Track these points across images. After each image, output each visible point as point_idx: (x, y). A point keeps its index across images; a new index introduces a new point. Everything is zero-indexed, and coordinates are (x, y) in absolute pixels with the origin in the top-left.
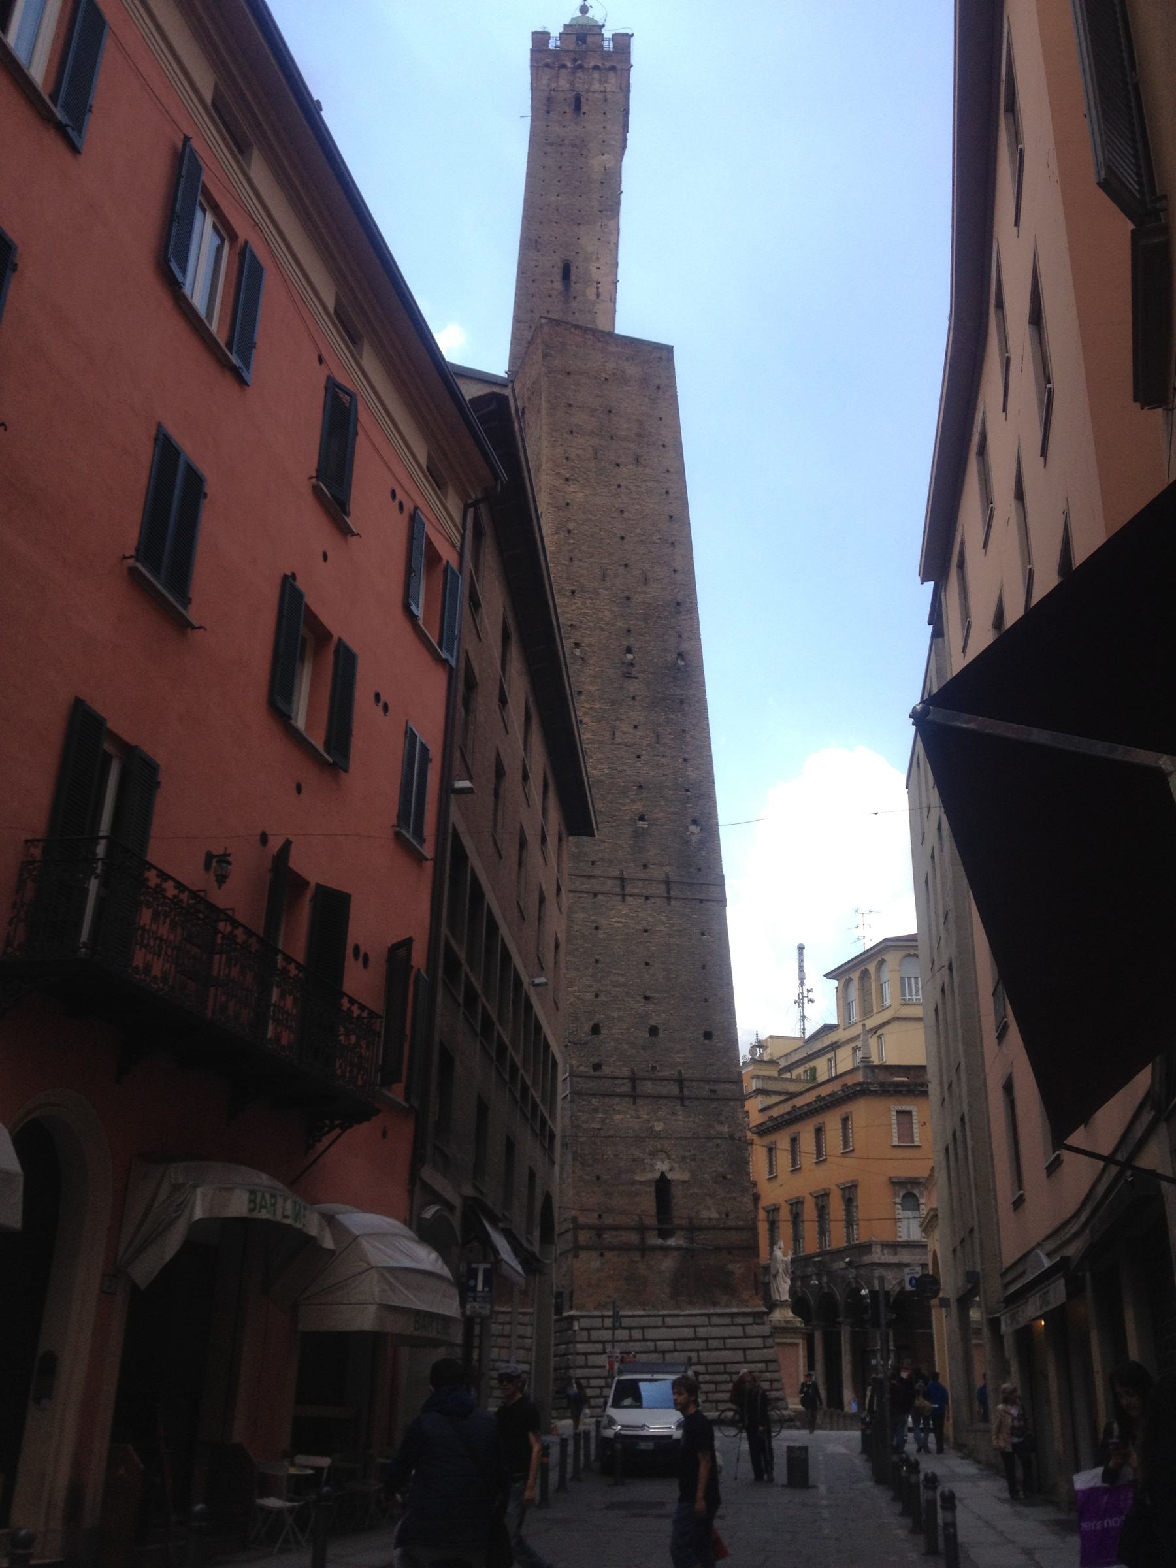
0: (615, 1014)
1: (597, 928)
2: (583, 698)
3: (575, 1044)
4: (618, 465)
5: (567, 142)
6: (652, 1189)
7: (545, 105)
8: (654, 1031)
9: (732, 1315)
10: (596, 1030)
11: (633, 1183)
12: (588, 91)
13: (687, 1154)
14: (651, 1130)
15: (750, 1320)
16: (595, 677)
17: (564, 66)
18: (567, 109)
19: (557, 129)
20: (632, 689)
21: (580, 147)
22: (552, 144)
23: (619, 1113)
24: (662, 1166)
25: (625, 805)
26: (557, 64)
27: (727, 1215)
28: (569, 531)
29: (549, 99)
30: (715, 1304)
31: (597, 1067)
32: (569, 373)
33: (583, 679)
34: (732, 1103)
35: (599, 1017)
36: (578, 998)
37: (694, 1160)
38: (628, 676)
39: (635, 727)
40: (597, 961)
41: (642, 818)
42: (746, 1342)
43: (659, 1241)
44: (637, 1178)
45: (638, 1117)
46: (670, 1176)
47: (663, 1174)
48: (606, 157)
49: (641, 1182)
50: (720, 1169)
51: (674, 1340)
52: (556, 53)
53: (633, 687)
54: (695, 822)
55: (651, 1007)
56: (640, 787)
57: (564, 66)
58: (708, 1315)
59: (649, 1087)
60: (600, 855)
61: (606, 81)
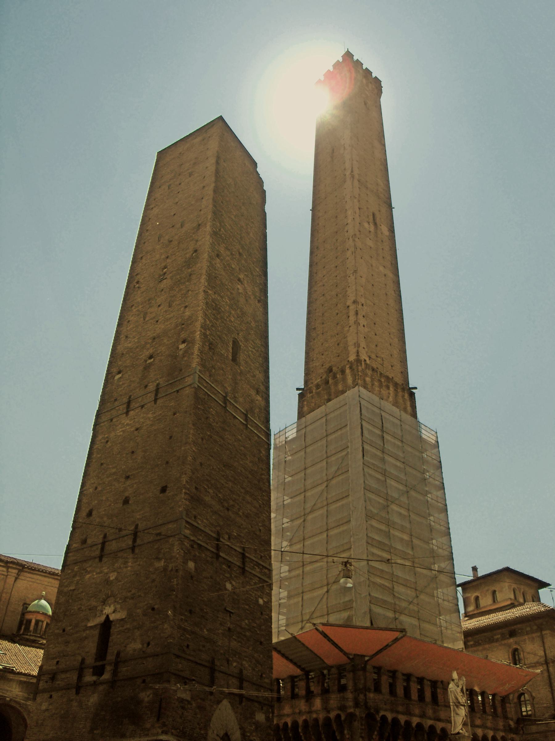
1: (107, 442)
2: (133, 308)
6: (96, 632)
8: (126, 501)
13: (129, 594)
14: (107, 582)
25: (141, 355)
27: (148, 644)
37: (132, 598)
39: (159, 306)
40: (102, 464)
41: (151, 357)
44: (90, 624)
45: (101, 572)
47: (108, 616)
50: (151, 602)
53: (163, 285)
55: (128, 482)
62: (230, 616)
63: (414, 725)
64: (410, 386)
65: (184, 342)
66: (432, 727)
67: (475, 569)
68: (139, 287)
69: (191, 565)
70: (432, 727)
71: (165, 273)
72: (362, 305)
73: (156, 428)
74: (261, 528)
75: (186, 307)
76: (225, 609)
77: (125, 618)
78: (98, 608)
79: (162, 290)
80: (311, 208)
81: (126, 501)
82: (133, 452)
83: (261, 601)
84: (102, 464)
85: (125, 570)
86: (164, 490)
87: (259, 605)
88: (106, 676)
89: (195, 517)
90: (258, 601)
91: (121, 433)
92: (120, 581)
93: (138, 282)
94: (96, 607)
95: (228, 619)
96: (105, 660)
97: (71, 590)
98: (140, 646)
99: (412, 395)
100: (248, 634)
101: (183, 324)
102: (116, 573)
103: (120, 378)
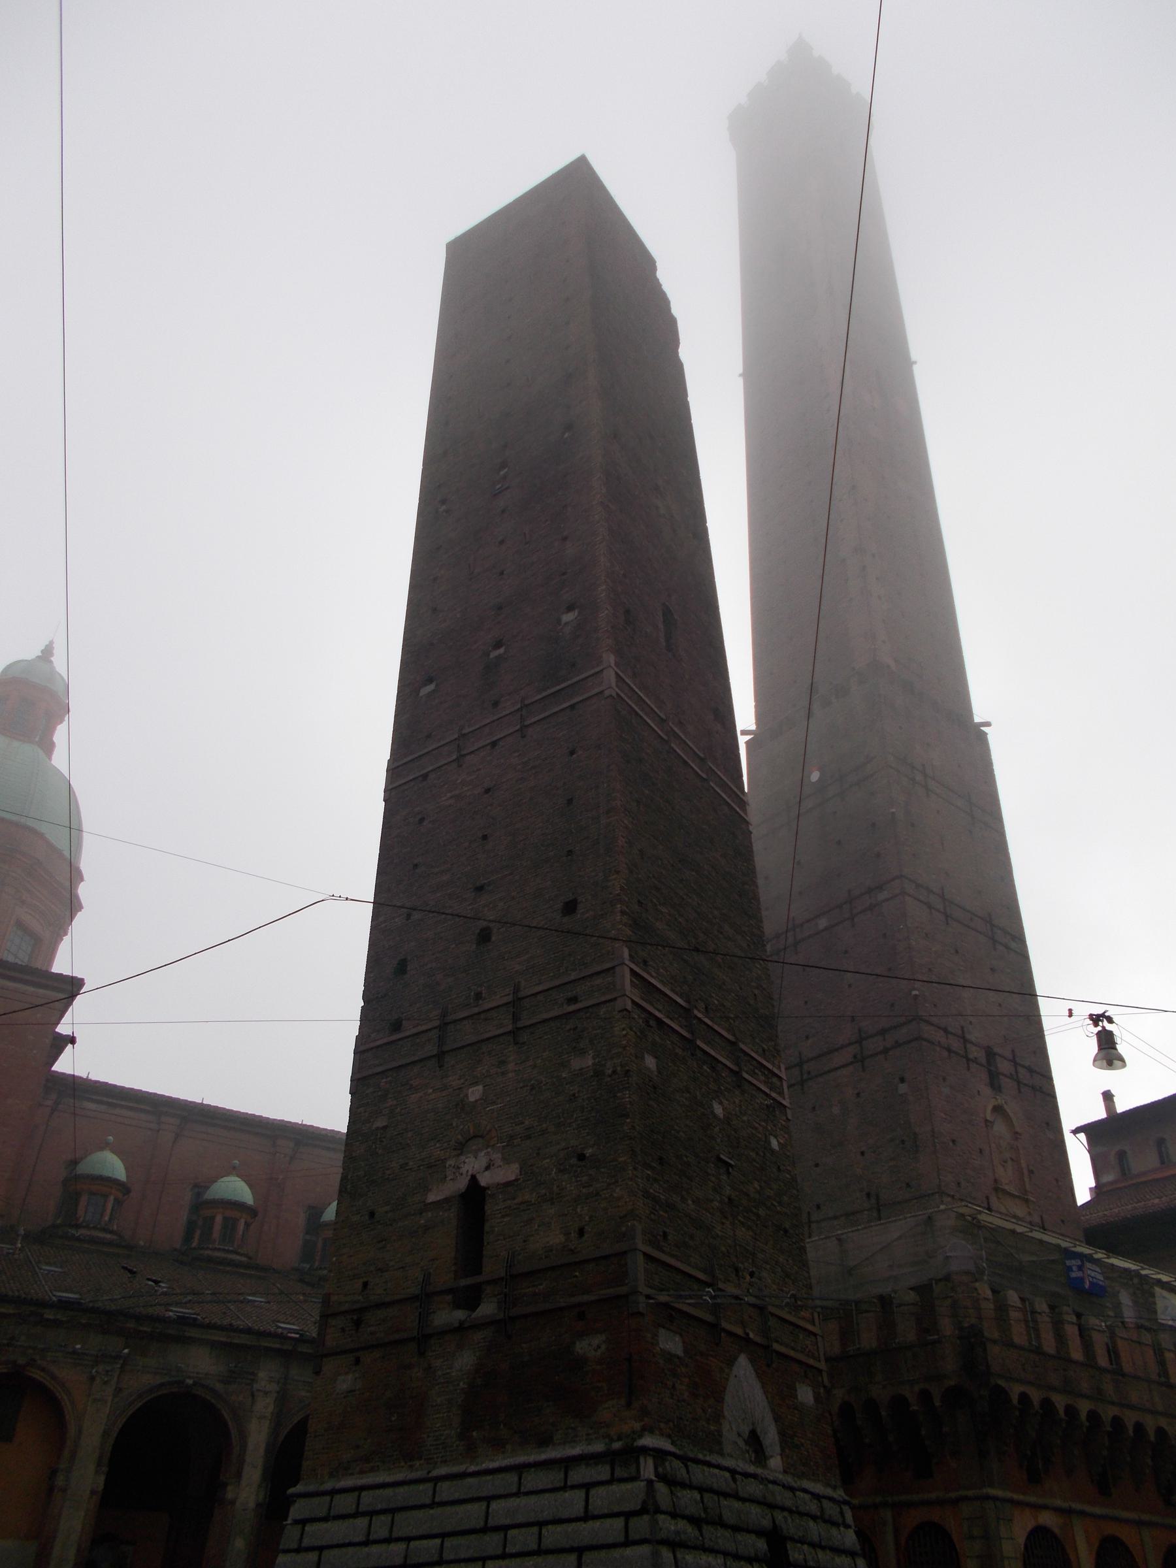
1: (422, 820)
8: (484, 937)
9: (567, 1463)
15: (602, 1472)
24: (472, 1164)
27: (581, 1232)
30: (545, 1441)
34: (602, 1011)
37: (529, 1137)
39: (502, 542)
40: (416, 866)
41: (498, 645)
42: (586, 1532)
43: (460, 1315)
44: (432, 1197)
46: (483, 1183)
47: (473, 1178)
49: (437, 1204)
58: (520, 1469)
62: (729, 1173)
63: (1083, 1416)
64: (977, 720)
65: (570, 609)
66: (1117, 1422)
67: (1108, 1097)
68: (447, 511)
69: (650, 1062)
70: (1117, 1422)
71: (505, 477)
72: (874, 556)
74: (756, 992)
75: (565, 539)
76: (719, 1159)
77: (516, 1180)
78: (448, 1163)
79: (503, 511)
80: (741, 371)
81: (484, 937)
82: (485, 837)
83: (774, 1144)
84: (416, 866)
86: (570, 907)
87: (773, 1151)
88: (487, 1309)
89: (645, 962)
90: (769, 1143)
92: (494, 1103)
93: (443, 502)
94: (444, 1161)
95: (724, 1177)
96: (480, 1273)
97: (377, 1128)
98: (562, 1238)
99: (982, 739)
100: (762, 1212)
101: (564, 574)
102: (480, 1088)
103: (434, 691)
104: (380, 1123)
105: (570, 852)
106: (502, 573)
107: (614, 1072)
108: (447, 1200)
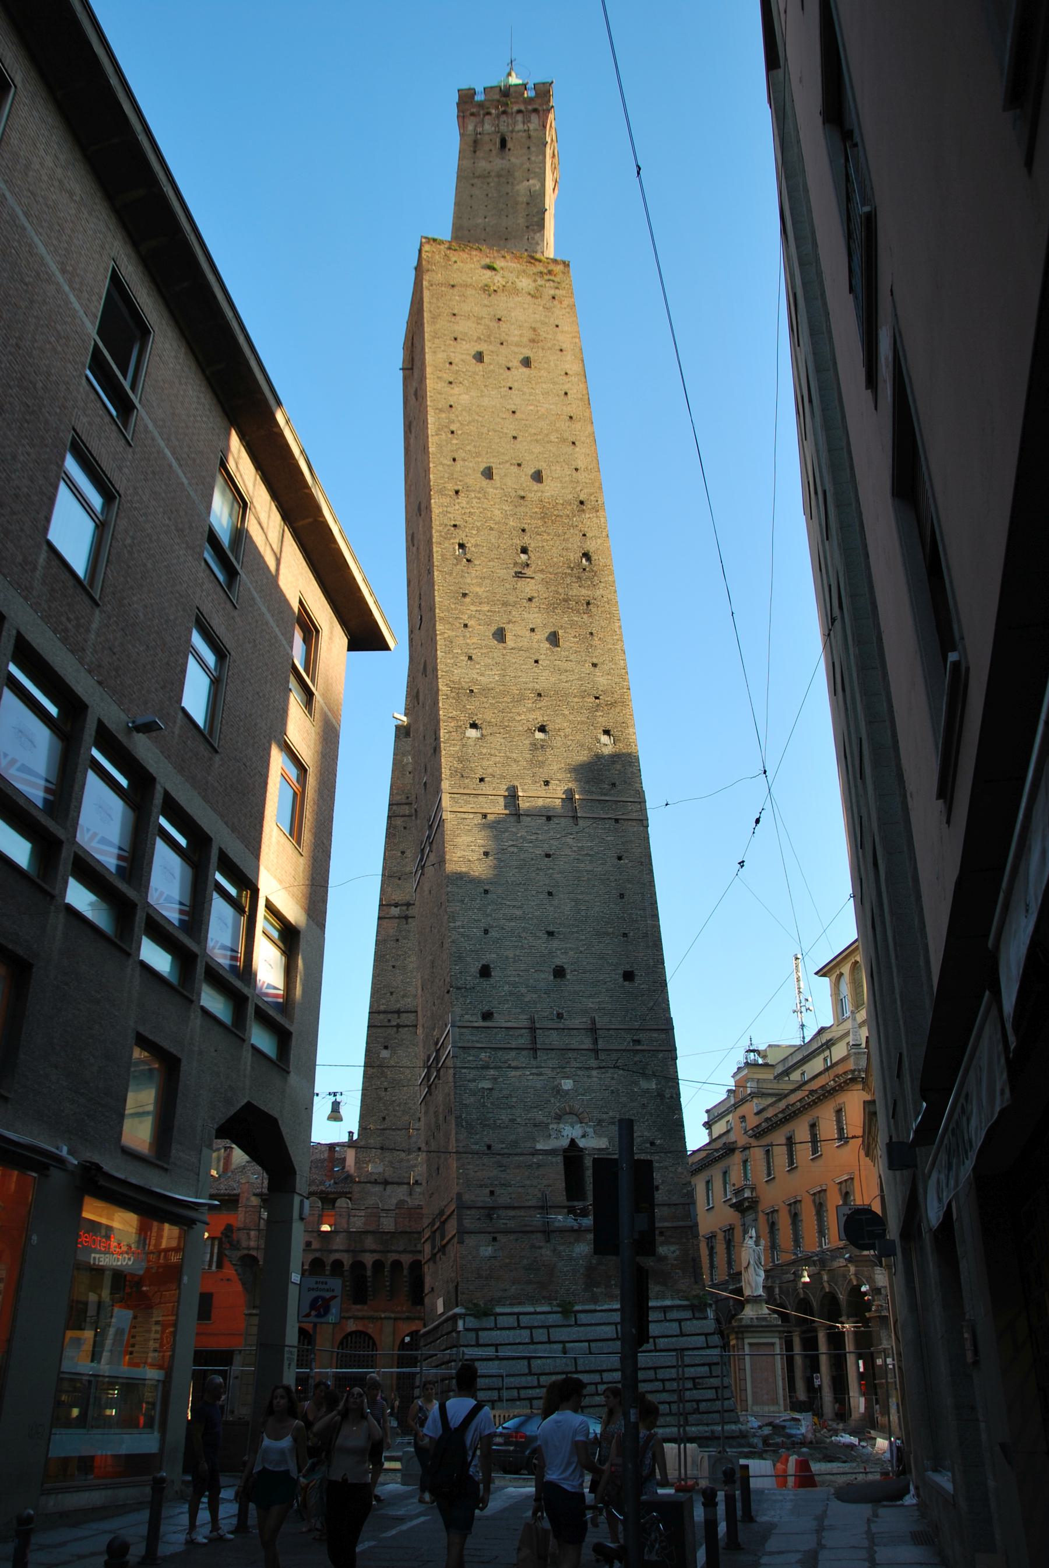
0: (510, 954)
2: (467, 600)
3: (458, 988)
4: (509, 369)
5: (493, 174)
6: (560, 1159)
7: (472, 146)
8: (559, 972)
10: (485, 972)
11: (536, 1152)
12: (512, 131)
13: (605, 1116)
14: (558, 1091)
16: (483, 578)
17: (489, 114)
18: (493, 148)
19: (482, 164)
20: (527, 590)
21: (506, 176)
22: (478, 177)
23: (516, 1068)
24: (571, 1131)
26: (482, 112)
28: (452, 432)
29: (475, 142)
31: (487, 1016)
32: (453, 286)
33: (468, 580)
34: (661, 1055)
35: (490, 957)
36: (463, 935)
38: (519, 575)
39: (533, 630)
40: (486, 892)
44: (539, 1147)
45: (540, 1074)
46: (581, 1145)
47: (573, 1141)
48: (531, 182)
49: (546, 1152)
50: (646, 1133)
51: (589, 1341)
52: (481, 105)
53: (528, 587)
54: (607, 732)
55: (555, 944)
56: (540, 695)
57: (489, 114)
59: (555, 1039)
60: (490, 771)
61: (529, 121)
73: (589, 868)
78: (551, 1127)
85: (586, 1079)
91: (515, 850)
92: (582, 1095)
104: (487, 1085)
105: (625, 935)
106: (536, 662)
107: (672, 1097)
108: (553, 1152)
